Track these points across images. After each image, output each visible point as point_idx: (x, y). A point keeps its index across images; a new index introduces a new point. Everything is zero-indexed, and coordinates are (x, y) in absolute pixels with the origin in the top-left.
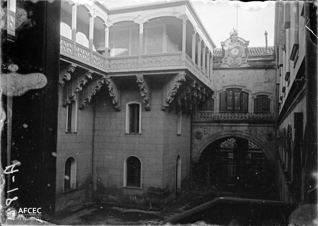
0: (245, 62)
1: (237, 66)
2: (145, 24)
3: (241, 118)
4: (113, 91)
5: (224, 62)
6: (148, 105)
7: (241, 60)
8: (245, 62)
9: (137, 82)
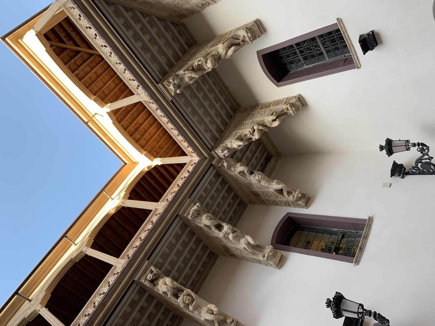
6: (242, 33)
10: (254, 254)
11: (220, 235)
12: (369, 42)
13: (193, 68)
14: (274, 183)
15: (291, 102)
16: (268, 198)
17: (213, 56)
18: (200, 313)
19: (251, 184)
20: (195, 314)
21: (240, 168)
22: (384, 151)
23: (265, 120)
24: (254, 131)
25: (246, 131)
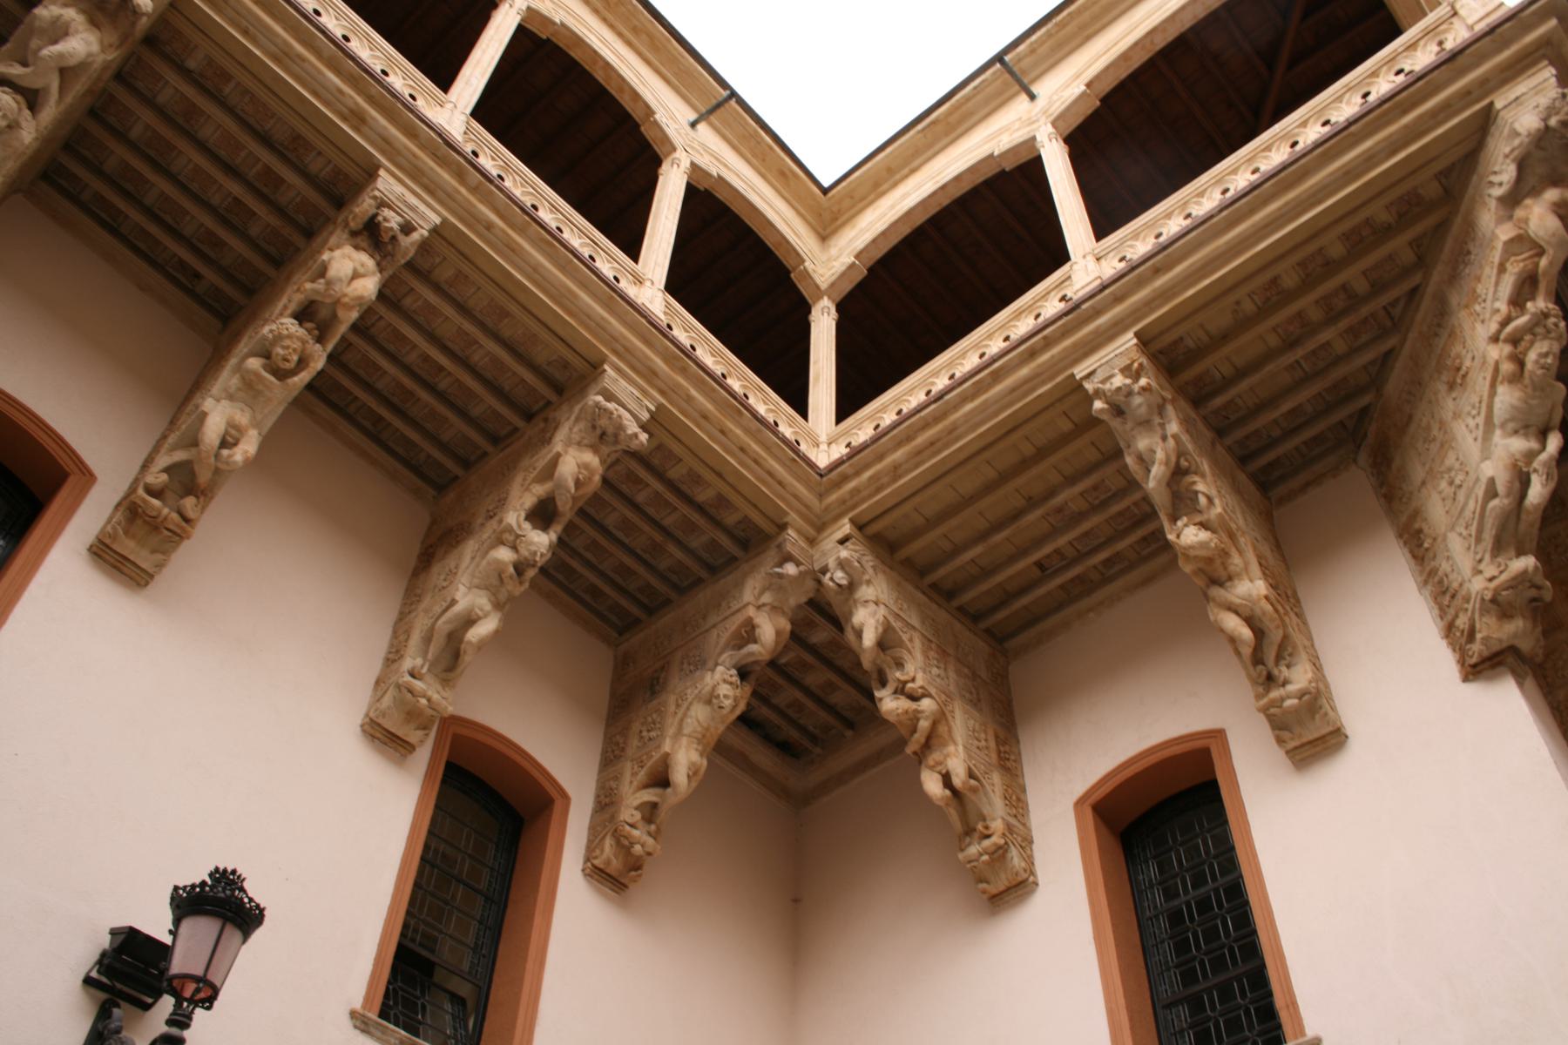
4: (910, 668)
6: (1299, 677)
10: (428, 639)
11: (514, 517)
13: (1186, 472)
14: (695, 756)
15: (1014, 853)
16: (636, 726)
17: (1225, 554)
18: (231, 398)
19: (701, 664)
20: (227, 378)
21: (769, 630)
23: (951, 748)
25: (916, 668)
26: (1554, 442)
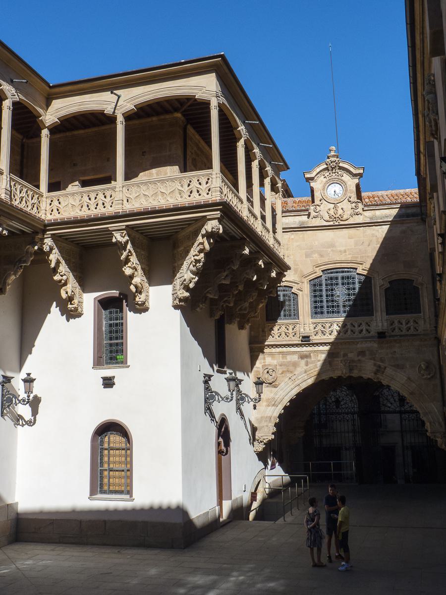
0: (357, 211)
1: (341, 220)
2: (128, 117)
3: (360, 333)
5: (313, 214)
7: (351, 207)
8: (357, 211)
9: (114, 240)
12: (108, 383)
22: (26, 376)
24: (62, 276)
25: (63, 268)
26: (197, 278)
